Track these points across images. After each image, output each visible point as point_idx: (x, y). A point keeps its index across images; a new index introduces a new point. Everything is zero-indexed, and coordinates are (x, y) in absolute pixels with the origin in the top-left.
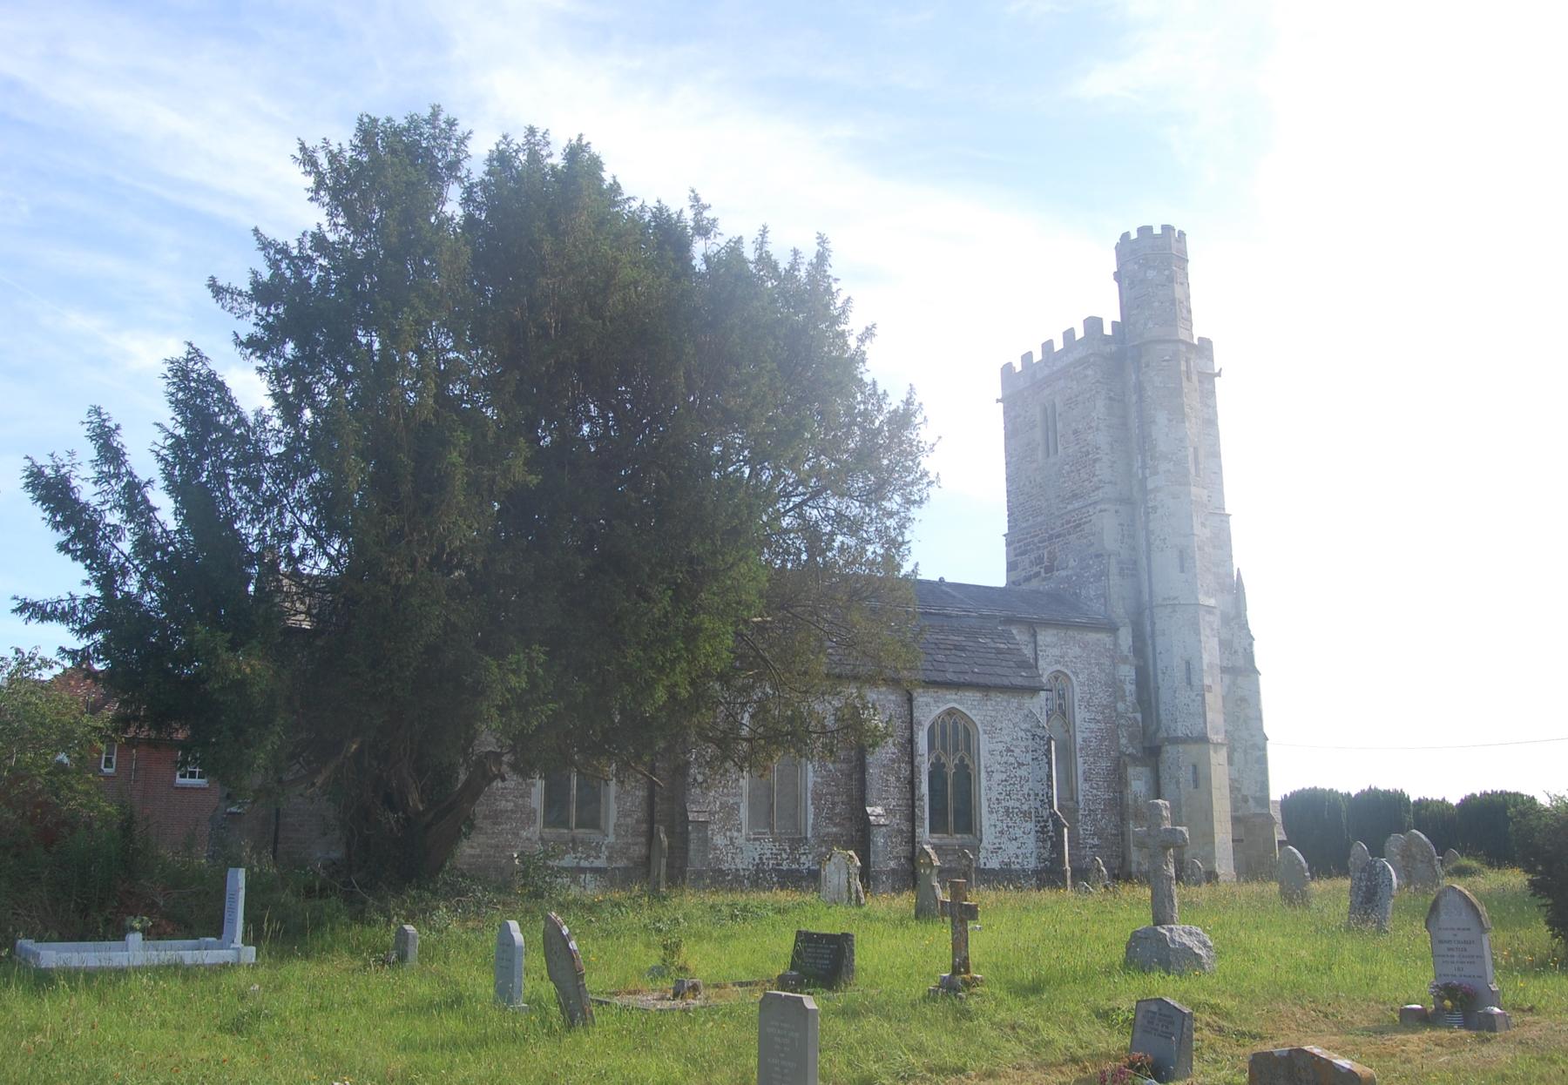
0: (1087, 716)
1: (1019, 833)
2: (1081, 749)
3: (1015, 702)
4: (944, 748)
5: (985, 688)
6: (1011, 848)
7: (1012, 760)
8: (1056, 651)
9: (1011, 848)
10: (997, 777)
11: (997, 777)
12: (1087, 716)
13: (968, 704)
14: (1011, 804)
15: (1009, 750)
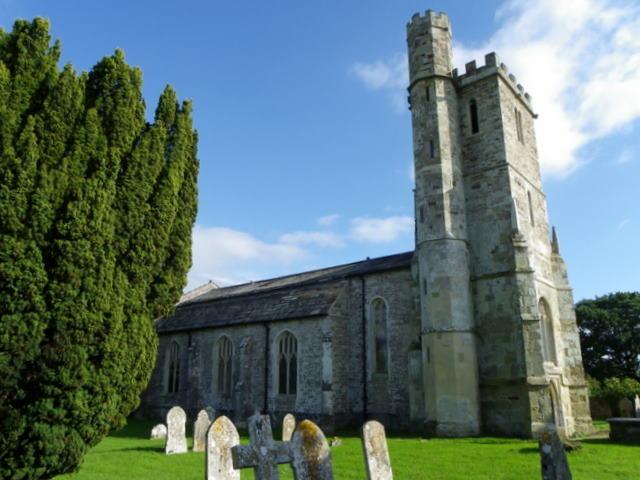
0: (394, 322)
1: (313, 393)
2: (390, 342)
3: (314, 324)
4: (286, 351)
5: (299, 319)
6: (310, 402)
7: (312, 355)
8: (376, 288)
9: (310, 402)
10: (305, 364)
11: (305, 364)
12: (394, 322)
13: (294, 328)
14: (310, 378)
15: (311, 349)
